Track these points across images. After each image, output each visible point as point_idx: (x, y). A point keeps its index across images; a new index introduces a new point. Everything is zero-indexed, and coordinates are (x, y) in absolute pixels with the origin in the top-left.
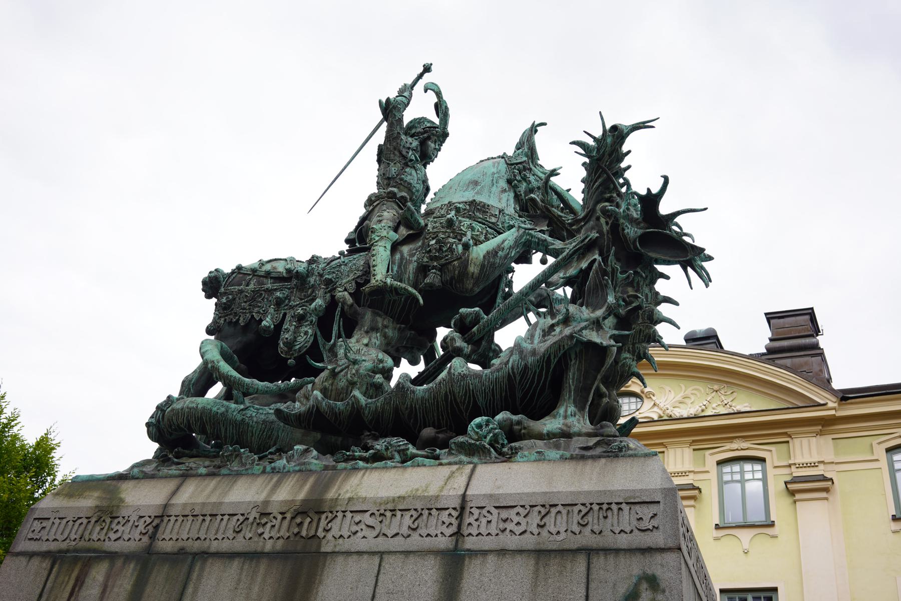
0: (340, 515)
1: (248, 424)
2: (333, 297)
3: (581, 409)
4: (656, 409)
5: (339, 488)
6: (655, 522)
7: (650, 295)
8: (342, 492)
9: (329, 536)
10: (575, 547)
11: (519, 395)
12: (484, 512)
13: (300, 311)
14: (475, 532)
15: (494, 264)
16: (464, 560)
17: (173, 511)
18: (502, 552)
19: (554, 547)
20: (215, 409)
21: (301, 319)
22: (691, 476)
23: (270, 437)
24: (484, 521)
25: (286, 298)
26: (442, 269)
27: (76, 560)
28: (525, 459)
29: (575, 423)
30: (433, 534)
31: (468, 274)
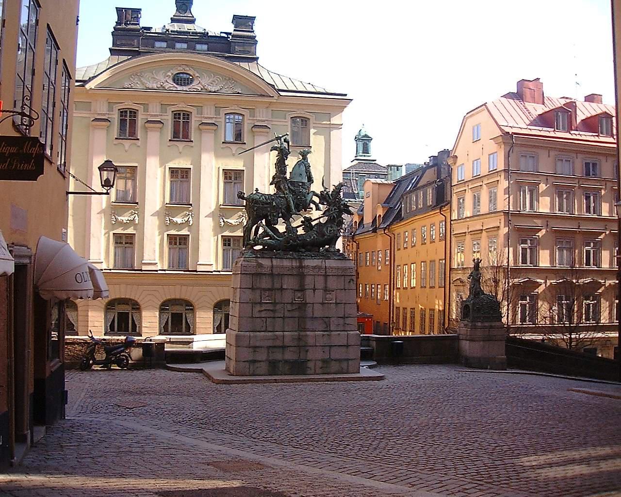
4: (199, 85)
22: (214, 119)
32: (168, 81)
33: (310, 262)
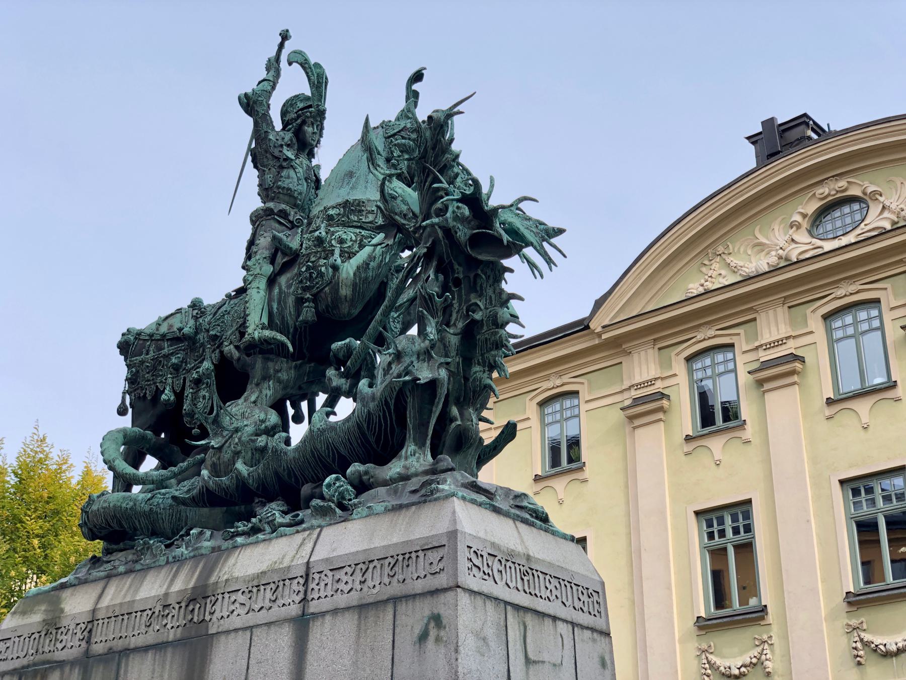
0: (220, 597)
1: (157, 512)
2: (222, 352)
3: (421, 445)
4: (886, 214)
5: (220, 571)
6: (441, 566)
7: (493, 296)
8: (221, 575)
9: (214, 618)
10: (385, 598)
11: (372, 440)
12: (323, 575)
13: (195, 376)
14: (316, 597)
15: (366, 278)
16: (309, 623)
17: (100, 615)
18: (335, 611)
19: (371, 600)
20: (124, 505)
21: (198, 382)
23: (179, 519)
24: (322, 584)
25: (182, 362)
26: (315, 298)
27: (36, 672)
28: (359, 515)
29: (415, 463)
30: (287, 604)
31: (340, 298)
32: (796, 237)
33: (250, 560)
